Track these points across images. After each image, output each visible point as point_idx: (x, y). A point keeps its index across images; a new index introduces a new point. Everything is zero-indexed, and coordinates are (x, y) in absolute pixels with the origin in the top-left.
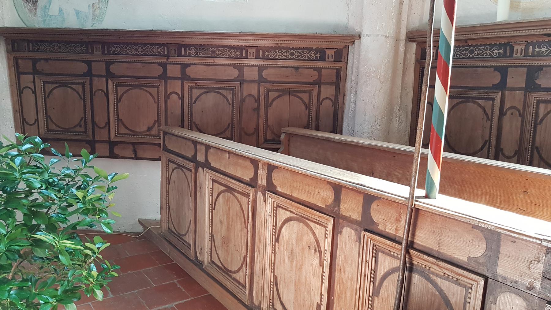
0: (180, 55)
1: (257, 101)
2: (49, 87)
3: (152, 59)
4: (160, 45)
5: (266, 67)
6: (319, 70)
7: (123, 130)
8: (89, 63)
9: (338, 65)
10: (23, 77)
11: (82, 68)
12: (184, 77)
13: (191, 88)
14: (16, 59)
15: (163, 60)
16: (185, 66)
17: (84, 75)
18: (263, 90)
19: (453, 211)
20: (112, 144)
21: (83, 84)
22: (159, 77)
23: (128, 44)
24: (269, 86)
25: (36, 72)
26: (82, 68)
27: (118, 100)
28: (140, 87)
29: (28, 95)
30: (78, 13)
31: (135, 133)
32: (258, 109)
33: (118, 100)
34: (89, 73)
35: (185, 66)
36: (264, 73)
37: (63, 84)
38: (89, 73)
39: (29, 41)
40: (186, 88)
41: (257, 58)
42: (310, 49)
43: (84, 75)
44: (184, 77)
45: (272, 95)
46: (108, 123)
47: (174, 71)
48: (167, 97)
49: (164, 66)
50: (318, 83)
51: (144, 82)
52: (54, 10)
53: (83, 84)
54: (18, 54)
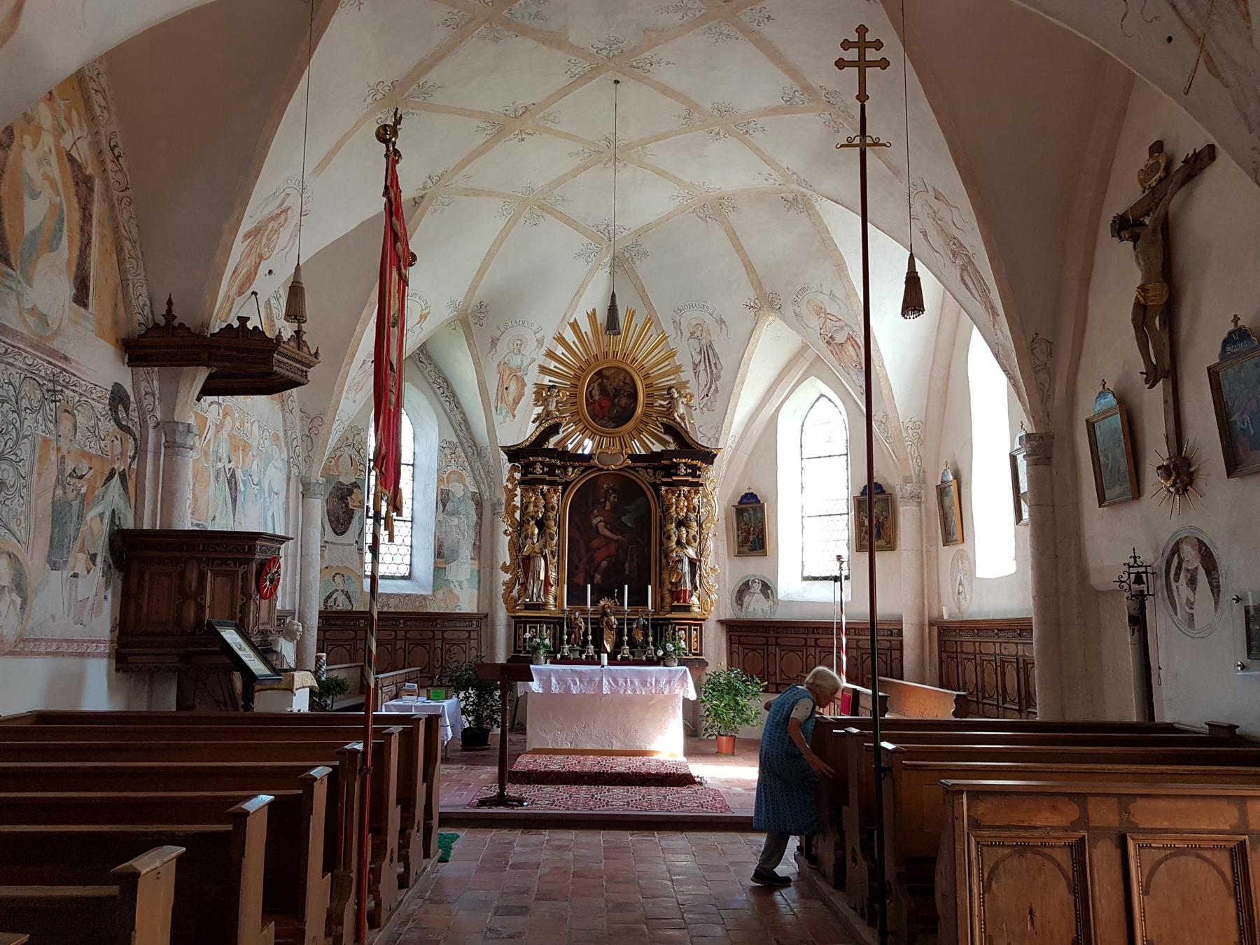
0: (814, 633)
1: (856, 660)
2: (746, 651)
3: (799, 636)
4: (803, 628)
5: (861, 640)
6: (890, 641)
7: (784, 677)
8: (767, 638)
9: (900, 638)
10: (733, 645)
11: (764, 641)
12: (816, 646)
13: (820, 652)
14: (731, 636)
15: (805, 636)
16: (816, 639)
17: (764, 645)
18: (859, 654)
19: (1092, 773)
20: (778, 685)
21: (763, 650)
22: (803, 646)
23: (787, 627)
24: (863, 651)
25: (740, 643)
26: (764, 641)
27: (782, 659)
28: (793, 651)
29: (735, 654)
30: (762, 610)
31: (790, 678)
32: (857, 665)
33: (782, 659)
34: (767, 644)
35: (816, 639)
36: (859, 643)
37: (753, 650)
38: (767, 644)
39: (737, 626)
40: (817, 651)
41: (856, 634)
42: (884, 629)
43: (764, 645)
44: (816, 646)
45: (865, 656)
46: (775, 673)
47: (811, 642)
48: (807, 657)
49: (805, 639)
50: (890, 649)
51: (796, 648)
52: (751, 609)
53: (763, 650)
54: (731, 633)
